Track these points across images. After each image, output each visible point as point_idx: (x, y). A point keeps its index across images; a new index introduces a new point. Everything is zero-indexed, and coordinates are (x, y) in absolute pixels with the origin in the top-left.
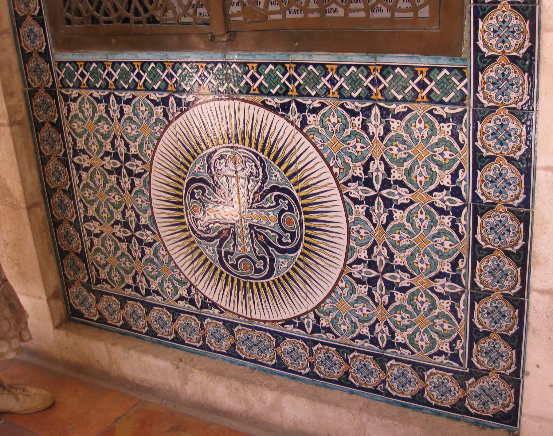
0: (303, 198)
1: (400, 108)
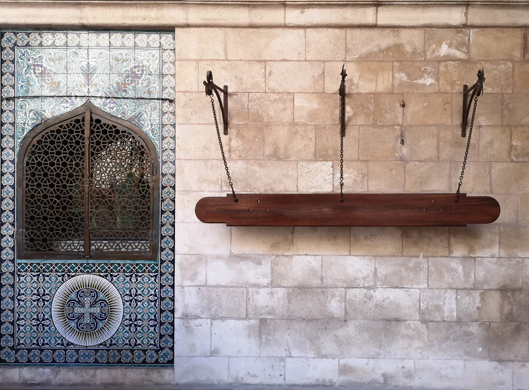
0: (109, 302)
1: (141, 274)
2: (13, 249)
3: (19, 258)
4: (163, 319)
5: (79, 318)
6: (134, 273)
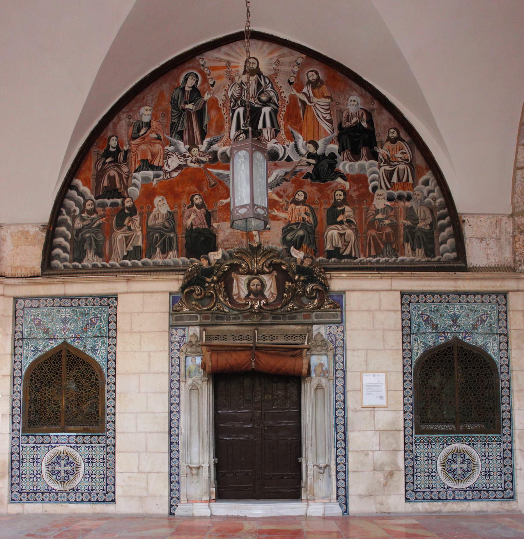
2: (412, 428)
3: (416, 433)
4: (506, 471)
5: (454, 471)
6: (486, 442)
